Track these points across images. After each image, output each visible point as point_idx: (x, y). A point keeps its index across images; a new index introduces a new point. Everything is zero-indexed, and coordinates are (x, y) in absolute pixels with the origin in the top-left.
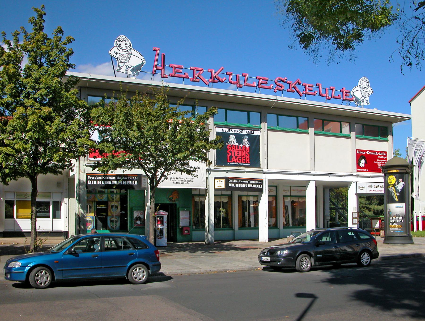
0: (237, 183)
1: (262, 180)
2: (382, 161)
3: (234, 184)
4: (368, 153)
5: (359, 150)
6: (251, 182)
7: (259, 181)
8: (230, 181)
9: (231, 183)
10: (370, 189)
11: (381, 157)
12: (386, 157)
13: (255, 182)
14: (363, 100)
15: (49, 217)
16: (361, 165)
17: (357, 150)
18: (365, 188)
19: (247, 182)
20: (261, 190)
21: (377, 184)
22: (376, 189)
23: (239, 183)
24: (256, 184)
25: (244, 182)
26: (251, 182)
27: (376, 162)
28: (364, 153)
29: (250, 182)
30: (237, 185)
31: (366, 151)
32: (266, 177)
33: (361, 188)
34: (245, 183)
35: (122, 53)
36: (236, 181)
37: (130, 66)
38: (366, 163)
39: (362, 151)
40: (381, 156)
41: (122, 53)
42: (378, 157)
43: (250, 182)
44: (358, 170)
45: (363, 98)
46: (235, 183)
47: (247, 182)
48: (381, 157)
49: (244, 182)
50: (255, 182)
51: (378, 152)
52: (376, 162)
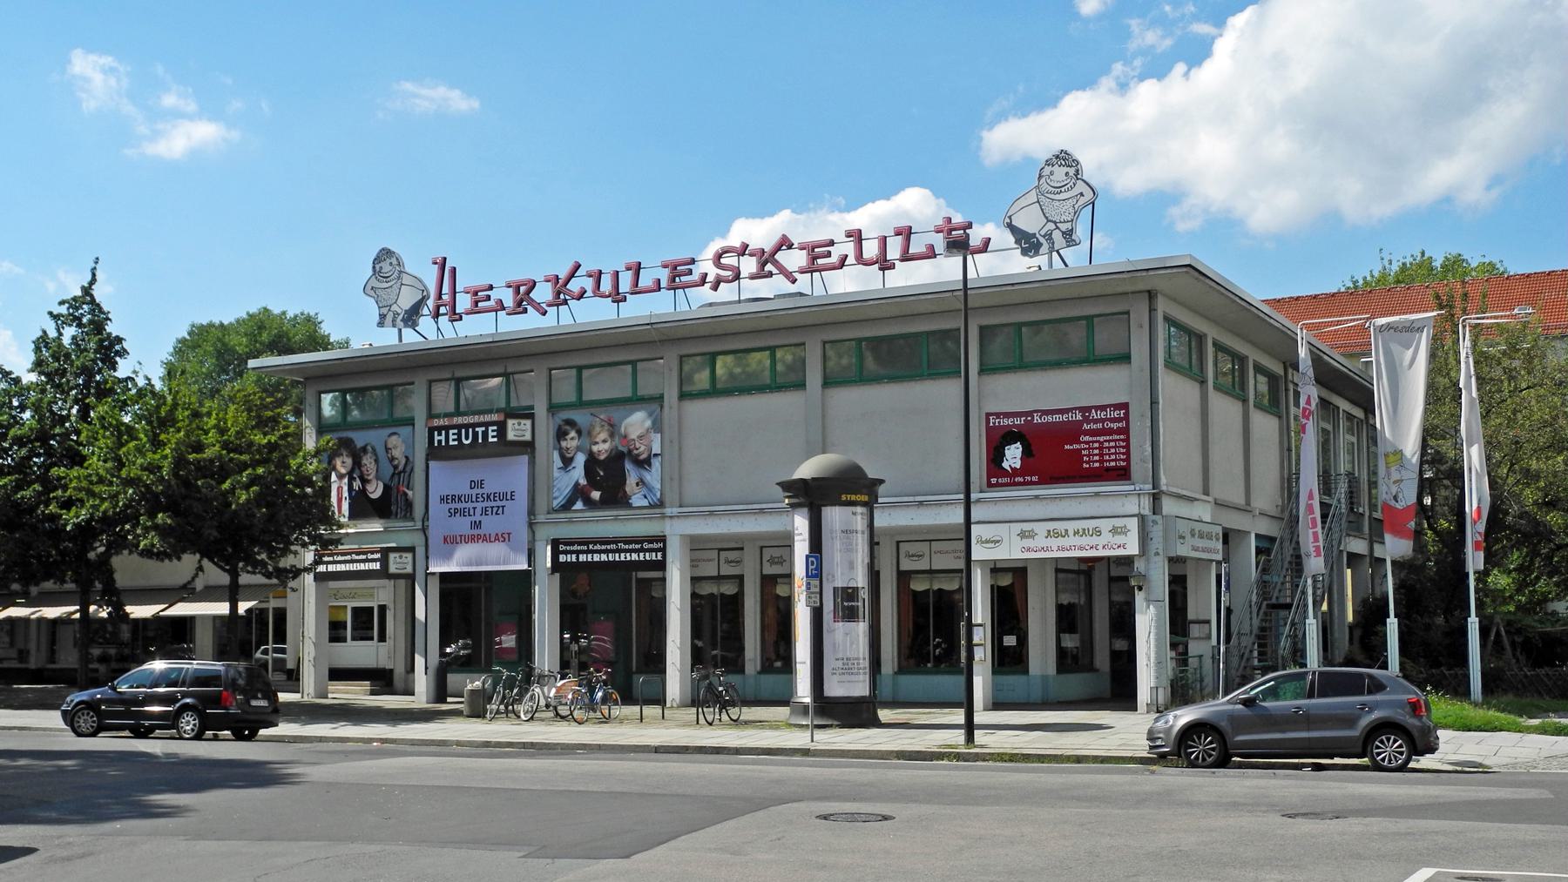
1: (662, 539)
4: (1037, 419)
5: (998, 415)
7: (651, 542)
8: (562, 548)
9: (566, 552)
10: (1028, 543)
14: (1049, 236)
16: (1005, 465)
17: (988, 415)
19: (613, 546)
20: (661, 565)
21: (1060, 526)
22: (1055, 543)
23: (587, 552)
24: (642, 550)
27: (1076, 446)
30: (582, 558)
31: (1030, 413)
34: (606, 552)
38: (1027, 453)
39: (1007, 415)
40: (1096, 421)
44: (994, 480)
45: (1051, 226)
46: (578, 553)
47: (613, 546)
48: (1100, 426)
51: (1084, 410)
52: (1076, 446)
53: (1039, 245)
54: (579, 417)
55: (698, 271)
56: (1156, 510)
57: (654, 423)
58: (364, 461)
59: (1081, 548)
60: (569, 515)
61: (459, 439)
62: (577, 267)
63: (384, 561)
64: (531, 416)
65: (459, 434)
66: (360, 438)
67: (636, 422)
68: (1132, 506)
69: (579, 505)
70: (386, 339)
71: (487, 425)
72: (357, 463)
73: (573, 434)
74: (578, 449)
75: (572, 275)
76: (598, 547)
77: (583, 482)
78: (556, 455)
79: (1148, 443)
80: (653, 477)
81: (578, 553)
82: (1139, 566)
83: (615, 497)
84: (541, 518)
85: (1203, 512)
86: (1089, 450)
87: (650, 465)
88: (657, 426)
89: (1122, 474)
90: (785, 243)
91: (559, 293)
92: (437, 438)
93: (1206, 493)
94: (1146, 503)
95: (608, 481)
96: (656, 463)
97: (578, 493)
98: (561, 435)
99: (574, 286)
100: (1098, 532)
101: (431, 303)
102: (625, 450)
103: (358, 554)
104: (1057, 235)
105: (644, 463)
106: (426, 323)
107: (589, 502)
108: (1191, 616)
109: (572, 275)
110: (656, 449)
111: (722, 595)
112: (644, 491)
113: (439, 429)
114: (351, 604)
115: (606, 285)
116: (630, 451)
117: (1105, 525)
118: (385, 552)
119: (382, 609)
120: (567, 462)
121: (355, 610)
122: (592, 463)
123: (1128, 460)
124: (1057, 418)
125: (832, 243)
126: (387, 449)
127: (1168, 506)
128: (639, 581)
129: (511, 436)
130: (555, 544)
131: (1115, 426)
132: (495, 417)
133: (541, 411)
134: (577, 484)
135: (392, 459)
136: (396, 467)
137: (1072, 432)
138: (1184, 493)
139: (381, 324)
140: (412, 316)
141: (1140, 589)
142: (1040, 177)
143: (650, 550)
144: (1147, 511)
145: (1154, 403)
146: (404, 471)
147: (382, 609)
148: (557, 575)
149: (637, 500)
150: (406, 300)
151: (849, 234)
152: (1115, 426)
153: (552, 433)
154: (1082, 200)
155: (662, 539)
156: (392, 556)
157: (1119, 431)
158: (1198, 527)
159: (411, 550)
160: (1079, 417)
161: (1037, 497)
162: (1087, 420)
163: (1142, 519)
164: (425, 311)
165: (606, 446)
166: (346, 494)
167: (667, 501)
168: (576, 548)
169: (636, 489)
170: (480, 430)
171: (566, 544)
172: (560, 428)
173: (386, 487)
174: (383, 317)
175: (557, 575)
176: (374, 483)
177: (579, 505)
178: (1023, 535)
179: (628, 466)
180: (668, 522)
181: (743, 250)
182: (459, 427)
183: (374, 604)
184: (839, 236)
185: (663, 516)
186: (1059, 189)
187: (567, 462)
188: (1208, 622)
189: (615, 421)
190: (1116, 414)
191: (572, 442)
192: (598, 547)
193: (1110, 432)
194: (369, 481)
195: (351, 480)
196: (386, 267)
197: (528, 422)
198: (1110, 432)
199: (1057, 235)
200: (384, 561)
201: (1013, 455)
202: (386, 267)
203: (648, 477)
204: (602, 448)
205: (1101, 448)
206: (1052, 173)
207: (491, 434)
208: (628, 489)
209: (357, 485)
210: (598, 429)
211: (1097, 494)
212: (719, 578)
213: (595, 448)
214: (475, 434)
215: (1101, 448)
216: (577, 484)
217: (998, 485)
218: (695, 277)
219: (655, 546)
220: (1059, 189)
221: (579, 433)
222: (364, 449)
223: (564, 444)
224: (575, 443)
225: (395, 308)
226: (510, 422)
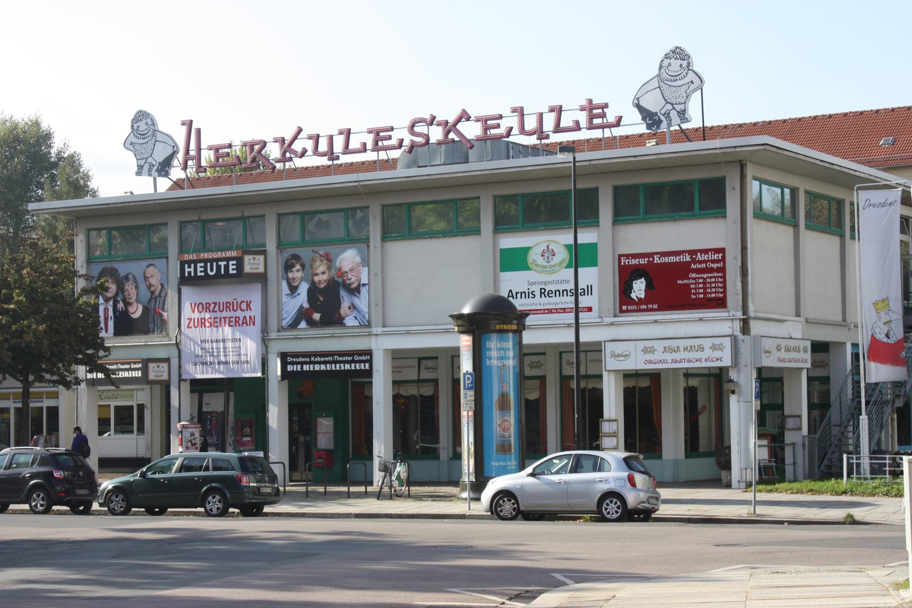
0: (306, 363)
1: (369, 353)
2: (705, 276)
3: (299, 366)
4: (657, 260)
5: (627, 256)
8: (289, 359)
9: (293, 363)
11: (703, 265)
12: (720, 265)
14: (667, 115)
15: (132, 432)
16: (633, 296)
17: (620, 256)
18: (633, 355)
19: (330, 359)
20: (369, 373)
22: (669, 357)
23: (310, 363)
25: (323, 359)
27: (686, 282)
28: (644, 261)
29: (337, 358)
31: (651, 255)
32: (381, 345)
33: (619, 356)
34: (325, 363)
35: (142, 141)
37: (154, 163)
39: (635, 256)
40: (701, 262)
41: (142, 141)
42: (693, 266)
43: (337, 358)
44: (624, 308)
45: (669, 107)
46: (302, 363)
47: (330, 359)
48: (703, 265)
49: (323, 359)
51: (692, 253)
52: (686, 282)
53: (660, 121)
54: (301, 252)
55: (396, 136)
56: (745, 330)
57: (363, 259)
58: (127, 287)
59: (689, 361)
60: (295, 333)
61: (205, 271)
62: (300, 130)
63: (145, 370)
64: (264, 253)
65: (205, 267)
66: (123, 269)
67: (348, 258)
68: (725, 328)
69: (303, 325)
70: (144, 187)
71: (228, 260)
72: (121, 289)
73: (298, 267)
74: (302, 279)
75: (295, 138)
76: (318, 359)
77: (306, 305)
78: (284, 284)
79: (739, 280)
80: (362, 302)
81: (302, 363)
82: (733, 375)
83: (332, 318)
84: (273, 335)
85: (795, 329)
86: (695, 283)
87: (359, 292)
88: (366, 262)
89: (720, 303)
90: (464, 116)
91: (285, 152)
92: (187, 270)
93: (798, 315)
94: (737, 325)
95: (326, 306)
96: (364, 290)
97: (303, 315)
98: (288, 267)
99: (297, 146)
100: (701, 349)
101: (180, 156)
102: (340, 280)
103: (123, 364)
104: (673, 114)
105: (355, 291)
106: (177, 173)
107: (312, 323)
108: (787, 412)
109: (295, 138)
110: (364, 280)
111: (421, 396)
112: (355, 313)
113: (189, 263)
114: (113, 404)
115: (323, 146)
116: (344, 281)
117: (707, 343)
118: (146, 362)
119: (141, 407)
120: (293, 289)
121: (116, 407)
122: (313, 291)
123: (725, 292)
124: (672, 259)
125: (501, 117)
126: (146, 278)
127: (756, 327)
128: (353, 383)
129: (247, 269)
130: (284, 356)
131: (715, 266)
132: (234, 254)
133: (271, 246)
135: (150, 286)
136: (153, 293)
137: (683, 269)
138: (773, 316)
139: (139, 173)
140: (164, 168)
141: (733, 392)
142: (661, 67)
143: (360, 362)
144: (738, 333)
145: (744, 249)
146: (160, 295)
147: (141, 407)
148: (286, 381)
149: (350, 321)
150: (160, 155)
151: (514, 110)
152: (715, 266)
153: (281, 268)
154: (692, 87)
155: (369, 353)
156: (151, 366)
157: (718, 270)
158: (783, 343)
159: (167, 360)
160: (688, 259)
161: (656, 322)
162: (694, 261)
163: (734, 339)
164: (176, 163)
165: (325, 277)
166: (111, 314)
167: (373, 324)
168: (301, 359)
170: (222, 264)
172: (287, 262)
173: (144, 307)
174: (140, 168)
175: (286, 381)
176: (135, 305)
177: (303, 325)
178: (646, 350)
179: (343, 293)
180: (373, 339)
181: (432, 121)
182: (205, 261)
183: (134, 403)
184: (506, 112)
185: (370, 335)
186: (675, 78)
187: (293, 289)
188: (800, 416)
189: (332, 257)
190: (715, 257)
191: (296, 274)
192: (318, 359)
193: (711, 270)
194: (130, 304)
195: (116, 303)
196: (142, 126)
197: (262, 258)
198: (711, 270)
199: (673, 114)
200: (145, 370)
201: (639, 288)
202: (142, 126)
203: (356, 301)
204: (322, 279)
205: (704, 283)
206: (670, 65)
207: (231, 267)
208: (342, 312)
209: (121, 305)
210: (318, 263)
211: (701, 319)
212: (419, 381)
213: (316, 279)
214: (219, 267)
215: (704, 283)
216: (301, 307)
217: (627, 311)
218: (394, 142)
219: (364, 358)
220: (675, 78)
221: (303, 266)
222: (126, 278)
223: (290, 275)
224: (299, 275)
225: (150, 160)
226: (247, 259)
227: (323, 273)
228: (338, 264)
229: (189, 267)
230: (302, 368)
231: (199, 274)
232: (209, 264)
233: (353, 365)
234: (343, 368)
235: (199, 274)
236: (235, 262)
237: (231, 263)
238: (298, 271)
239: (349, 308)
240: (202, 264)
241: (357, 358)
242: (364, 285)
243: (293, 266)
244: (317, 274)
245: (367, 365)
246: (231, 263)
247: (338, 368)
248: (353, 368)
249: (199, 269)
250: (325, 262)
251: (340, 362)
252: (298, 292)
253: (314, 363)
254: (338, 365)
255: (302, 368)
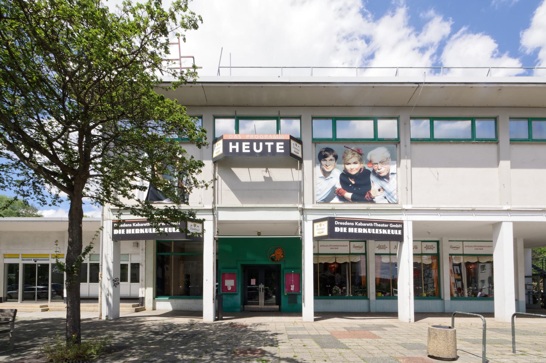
0: (351, 226)
1: (401, 223)
6: (379, 225)
7: (394, 223)
9: (339, 226)
13: (386, 226)
20: (400, 239)
23: (354, 227)
25: (365, 225)
26: (379, 225)
30: (351, 230)
34: (367, 227)
36: (348, 224)
46: (347, 227)
50: (386, 226)
69: (336, 200)
71: (275, 141)
73: (331, 157)
76: (361, 224)
77: (339, 186)
80: (391, 185)
87: (388, 179)
92: (231, 147)
97: (334, 193)
107: (343, 199)
113: (234, 142)
116: (374, 171)
122: (345, 177)
134: (334, 188)
143: (394, 229)
155: (401, 223)
168: (346, 223)
169: (379, 193)
171: (340, 221)
179: (372, 178)
182: (251, 141)
187: (326, 174)
189: (363, 152)
192: (361, 224)
207: (278, 147)
210: (350, 155)
213: (348, 167)
214: (265, 147)
219: (397, 226)
221: (336, 157)
227: (355, 163)
228: (368, 157)
229: (234, 144)
230: (347, 230)
231: (244, 151)
232: (255, 144)
233: (389, 231)
234: (381, 233)
235: (244, 151)
236: (282, 143)
237: (278, 144)
238: (331, 160)
239: (379, 190)
240: (248, 143)
241: (392, 226)
242: (392, 174)
243: (326, 156)
244: (349, 164)
245: (400, 232)
246: (278, 144)
247: (377, 232)
248: (389, 233)
249: (244, 147)
250: (356, 155)
251: (379, 228)
252: (331, 175)
253: (358, 227)
254: (377, 230)
255: (347, 230)
